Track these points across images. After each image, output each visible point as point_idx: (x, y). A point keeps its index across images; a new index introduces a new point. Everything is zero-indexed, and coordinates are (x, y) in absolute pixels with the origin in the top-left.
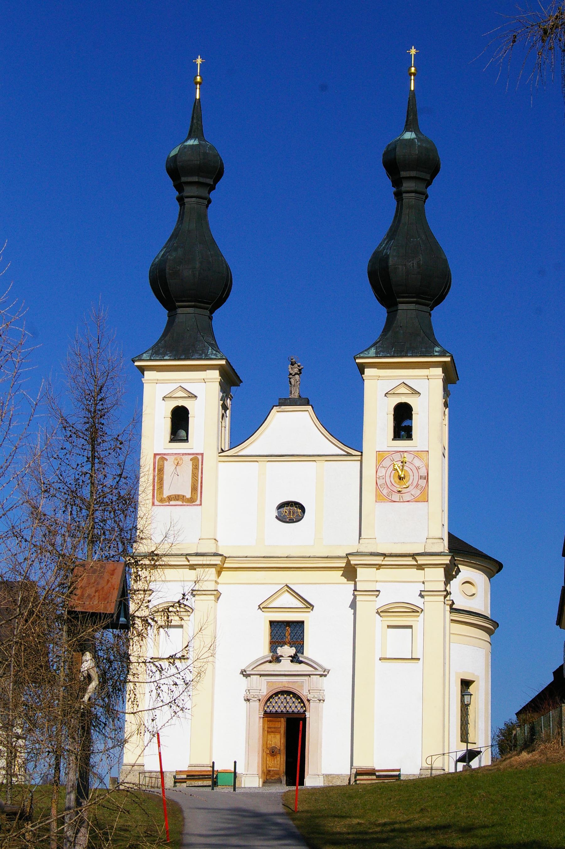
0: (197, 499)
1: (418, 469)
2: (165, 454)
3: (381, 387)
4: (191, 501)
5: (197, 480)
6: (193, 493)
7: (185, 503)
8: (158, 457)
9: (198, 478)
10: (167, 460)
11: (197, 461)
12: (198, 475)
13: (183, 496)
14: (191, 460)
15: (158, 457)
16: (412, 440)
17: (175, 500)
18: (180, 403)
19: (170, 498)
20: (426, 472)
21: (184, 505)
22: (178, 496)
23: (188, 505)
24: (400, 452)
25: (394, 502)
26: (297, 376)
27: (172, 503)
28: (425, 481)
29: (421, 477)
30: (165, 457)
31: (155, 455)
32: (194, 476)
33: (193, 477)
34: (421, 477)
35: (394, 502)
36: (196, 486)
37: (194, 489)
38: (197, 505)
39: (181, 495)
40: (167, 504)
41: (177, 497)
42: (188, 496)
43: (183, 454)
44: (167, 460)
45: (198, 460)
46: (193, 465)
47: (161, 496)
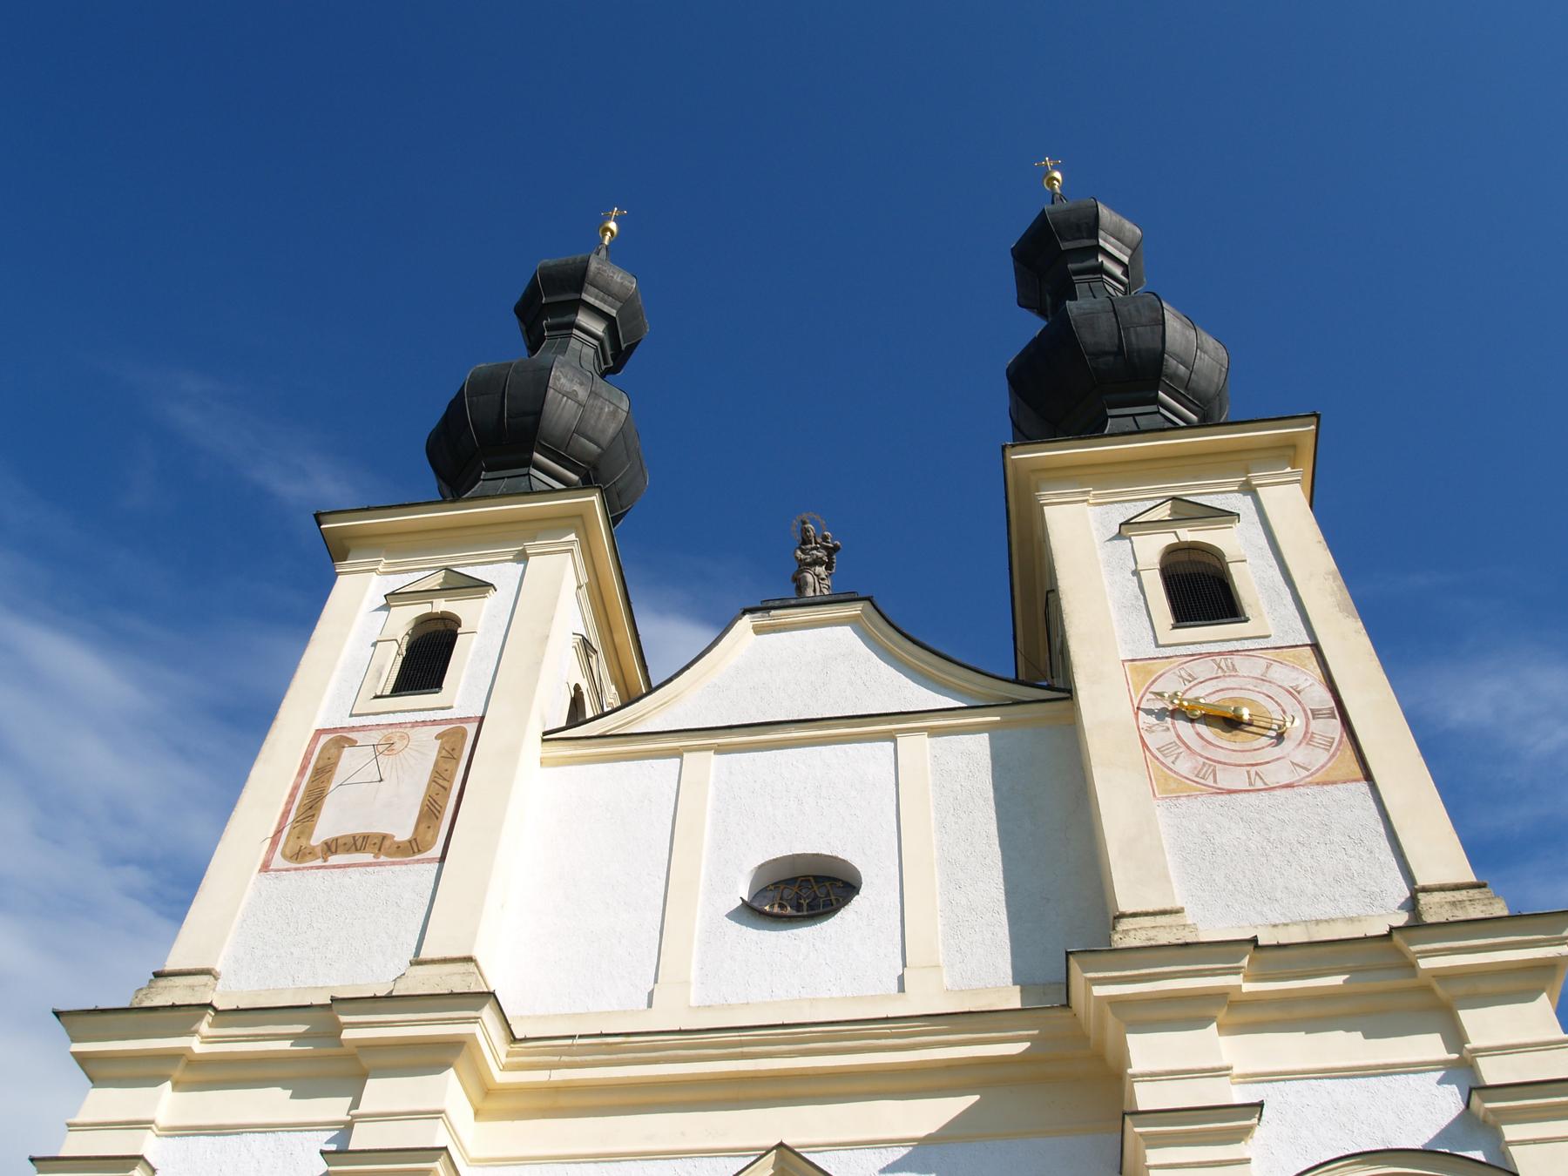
0: (433, 843)
1: (1294, 693)
2: (352, 729)
3: (1097, 546)
4: (412, 848)
5: (447, 790)
6: (423, 826)
7: (383, 858)
8: (324, 739)
9: (450, 781)
10: (353, 743)
11: (458, 746)
12: (453, 776)
13: (384, 837)
14: (438, 737)
15: (324, 739)
16: (1247, 620)
17: (348, 851)
18: (441, 605)
19: (331, 847)
20: (1328, 696)
21: (380, 864)
22: (366, 837)
23: (393, 863)
24: (1210, 654)
25: (1230, 792)
26: (821, 570)
27: (333, 860)
28: (1337, 722)
29: (1316, 714)
30: (350, 735)
31: (319, 732)
32: (440, 778)
33: (433, 781)
34: (1316, 714)
35: (1230, 792)
36: (439, 808)
37: (430, 812)
38: (430, 861)
39: (376, 835)
40: (319, 862)
41: (357, 843)
42: (403, 834)
43: (415, 724)
44: (353, 743)
45: (464, 734)
46: (442, 748)
47: (303, 842)
